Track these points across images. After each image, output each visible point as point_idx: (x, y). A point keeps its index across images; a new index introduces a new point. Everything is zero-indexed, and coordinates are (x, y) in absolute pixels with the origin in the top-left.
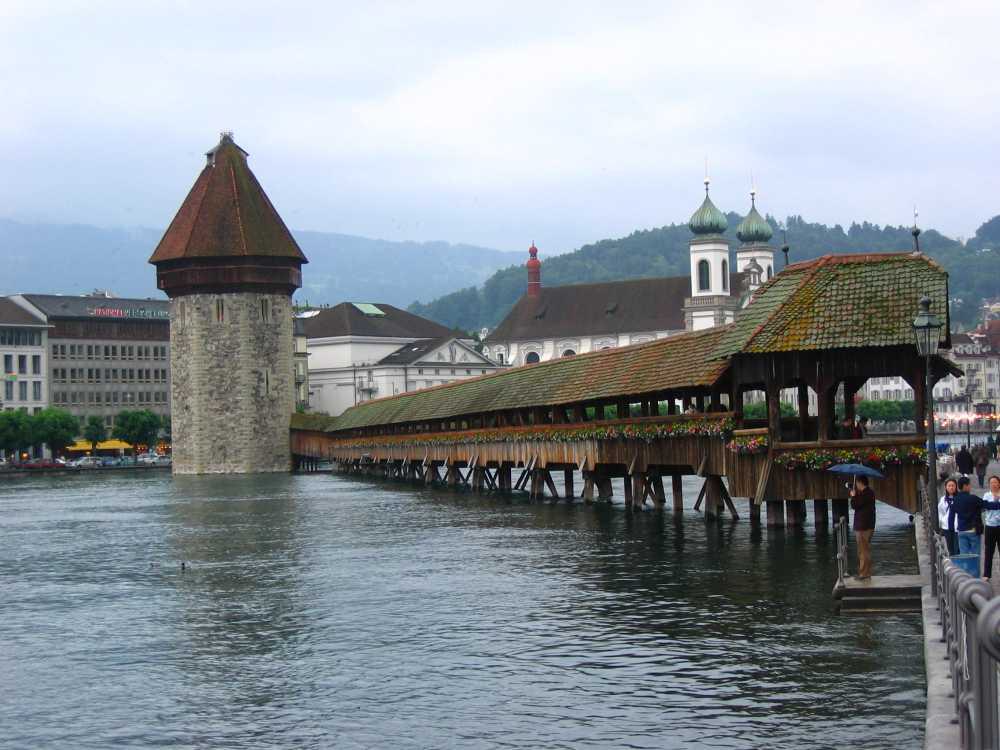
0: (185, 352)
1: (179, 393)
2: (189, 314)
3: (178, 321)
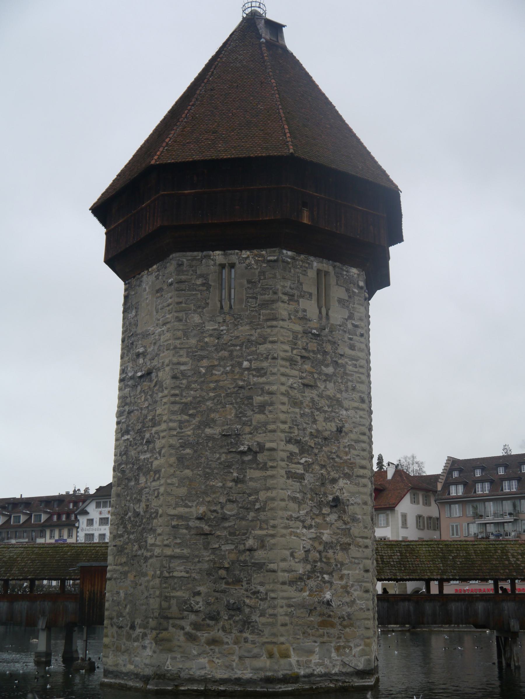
0: (328, 378)
1: (307, 466)
2: (340, 301)
3: (310, 307)
